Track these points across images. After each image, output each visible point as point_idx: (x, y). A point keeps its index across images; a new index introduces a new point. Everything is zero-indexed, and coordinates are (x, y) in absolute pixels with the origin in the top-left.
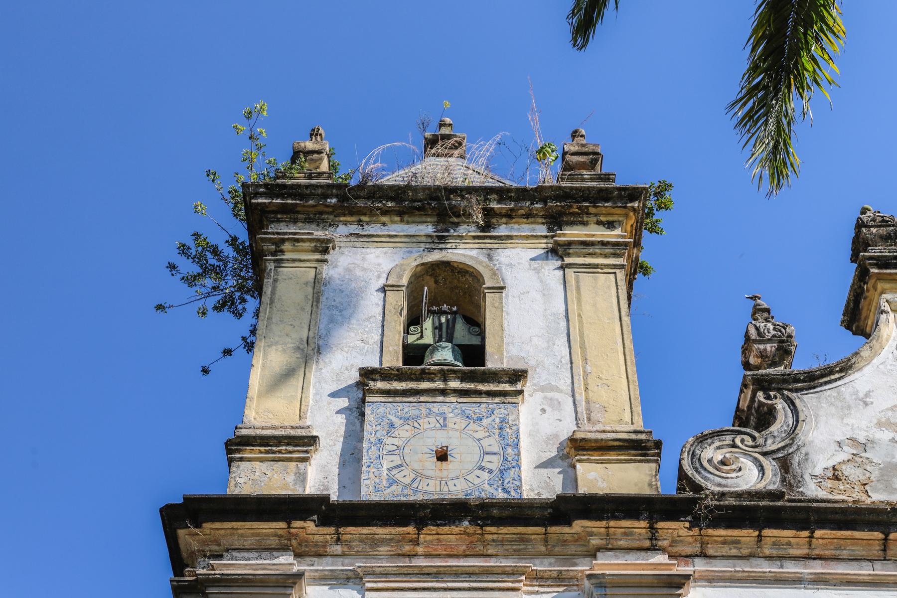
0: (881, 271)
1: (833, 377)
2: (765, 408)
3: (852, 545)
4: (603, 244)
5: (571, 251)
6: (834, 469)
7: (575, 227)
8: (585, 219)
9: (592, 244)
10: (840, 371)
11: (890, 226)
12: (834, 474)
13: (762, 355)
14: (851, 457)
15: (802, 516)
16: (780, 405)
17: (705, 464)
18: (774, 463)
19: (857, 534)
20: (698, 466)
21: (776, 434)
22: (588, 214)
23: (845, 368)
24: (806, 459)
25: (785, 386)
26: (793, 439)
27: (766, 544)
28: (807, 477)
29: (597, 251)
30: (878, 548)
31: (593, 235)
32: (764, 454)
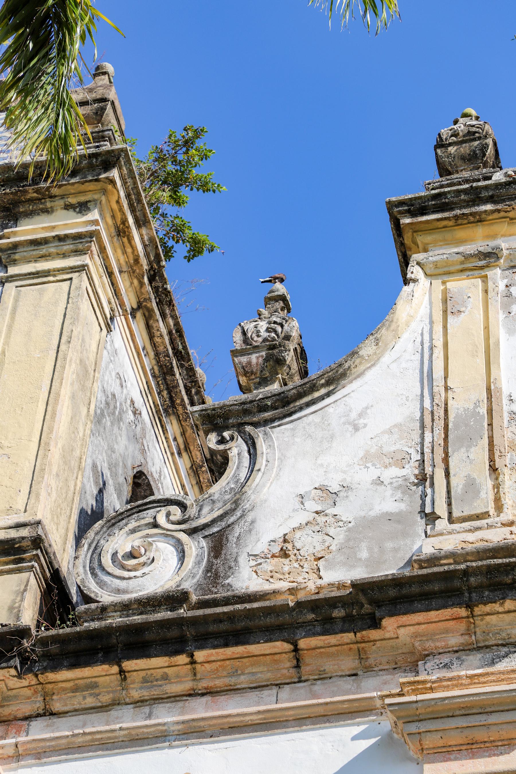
0: (415, 220)
1: (316, 395)
2: (219, 457)
3: (252, 665)
4: (60, 239)
5: (17, 256)
6: (285, 541)
7: (37, 218)
8: (49, 205)
9: (45, 241)
10: (328, 383)
11: (474, 140)
12: (282, 549)
13: (246, 371)
14: (310, 517)
15: (174, 633)
16: (237, 449)
17: (107, 561)
18: (204, 543)
19: (254, 649)
20: (96, 565)
21: (216, 497)
22: (52, 197)
23: (335, 379)
24: (250, 531)
25: (247, 419)
26: (236, 503)
27: (133, 682)
28: (243, 560)
29: (53, 250)
30: (288, 664)
31: (53, 228)
32: (192, 532)
